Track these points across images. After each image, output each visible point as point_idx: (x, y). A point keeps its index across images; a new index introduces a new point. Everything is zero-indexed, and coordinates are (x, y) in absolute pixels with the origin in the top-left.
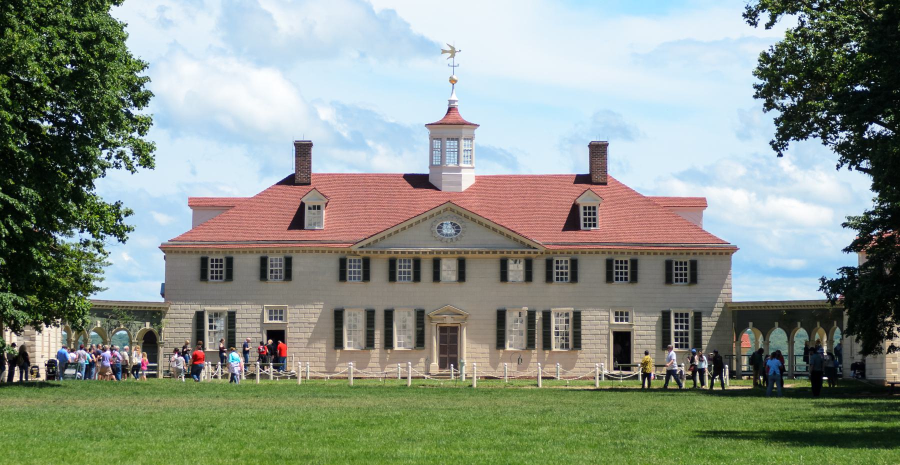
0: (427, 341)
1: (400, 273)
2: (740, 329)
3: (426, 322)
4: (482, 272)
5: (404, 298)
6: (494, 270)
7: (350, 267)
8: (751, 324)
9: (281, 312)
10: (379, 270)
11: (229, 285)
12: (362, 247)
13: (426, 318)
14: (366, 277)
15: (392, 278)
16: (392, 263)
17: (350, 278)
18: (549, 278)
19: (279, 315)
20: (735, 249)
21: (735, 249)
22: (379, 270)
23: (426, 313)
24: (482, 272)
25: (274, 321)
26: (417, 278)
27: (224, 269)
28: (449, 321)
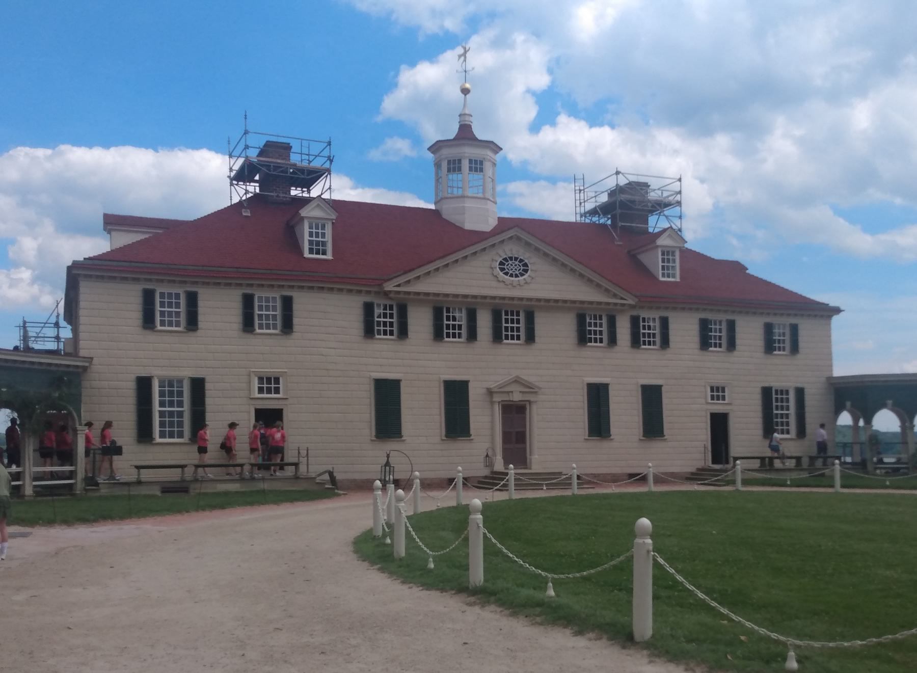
4: (556, 331)
6: (566, 326)
8: (848, 404)
9: (277, 380)
10: (420, 321)
11: (192, 338)
12: (399, 286)
14: (403, 332)
15: (438, 334)
16: (438, 313)
18: (636, 342)
20: (837, 311)
21: (837, 311)
22: (420, 321)
24: (556, 331)
26: (472, 336)
27: (158, 308)
28: (517, 397)
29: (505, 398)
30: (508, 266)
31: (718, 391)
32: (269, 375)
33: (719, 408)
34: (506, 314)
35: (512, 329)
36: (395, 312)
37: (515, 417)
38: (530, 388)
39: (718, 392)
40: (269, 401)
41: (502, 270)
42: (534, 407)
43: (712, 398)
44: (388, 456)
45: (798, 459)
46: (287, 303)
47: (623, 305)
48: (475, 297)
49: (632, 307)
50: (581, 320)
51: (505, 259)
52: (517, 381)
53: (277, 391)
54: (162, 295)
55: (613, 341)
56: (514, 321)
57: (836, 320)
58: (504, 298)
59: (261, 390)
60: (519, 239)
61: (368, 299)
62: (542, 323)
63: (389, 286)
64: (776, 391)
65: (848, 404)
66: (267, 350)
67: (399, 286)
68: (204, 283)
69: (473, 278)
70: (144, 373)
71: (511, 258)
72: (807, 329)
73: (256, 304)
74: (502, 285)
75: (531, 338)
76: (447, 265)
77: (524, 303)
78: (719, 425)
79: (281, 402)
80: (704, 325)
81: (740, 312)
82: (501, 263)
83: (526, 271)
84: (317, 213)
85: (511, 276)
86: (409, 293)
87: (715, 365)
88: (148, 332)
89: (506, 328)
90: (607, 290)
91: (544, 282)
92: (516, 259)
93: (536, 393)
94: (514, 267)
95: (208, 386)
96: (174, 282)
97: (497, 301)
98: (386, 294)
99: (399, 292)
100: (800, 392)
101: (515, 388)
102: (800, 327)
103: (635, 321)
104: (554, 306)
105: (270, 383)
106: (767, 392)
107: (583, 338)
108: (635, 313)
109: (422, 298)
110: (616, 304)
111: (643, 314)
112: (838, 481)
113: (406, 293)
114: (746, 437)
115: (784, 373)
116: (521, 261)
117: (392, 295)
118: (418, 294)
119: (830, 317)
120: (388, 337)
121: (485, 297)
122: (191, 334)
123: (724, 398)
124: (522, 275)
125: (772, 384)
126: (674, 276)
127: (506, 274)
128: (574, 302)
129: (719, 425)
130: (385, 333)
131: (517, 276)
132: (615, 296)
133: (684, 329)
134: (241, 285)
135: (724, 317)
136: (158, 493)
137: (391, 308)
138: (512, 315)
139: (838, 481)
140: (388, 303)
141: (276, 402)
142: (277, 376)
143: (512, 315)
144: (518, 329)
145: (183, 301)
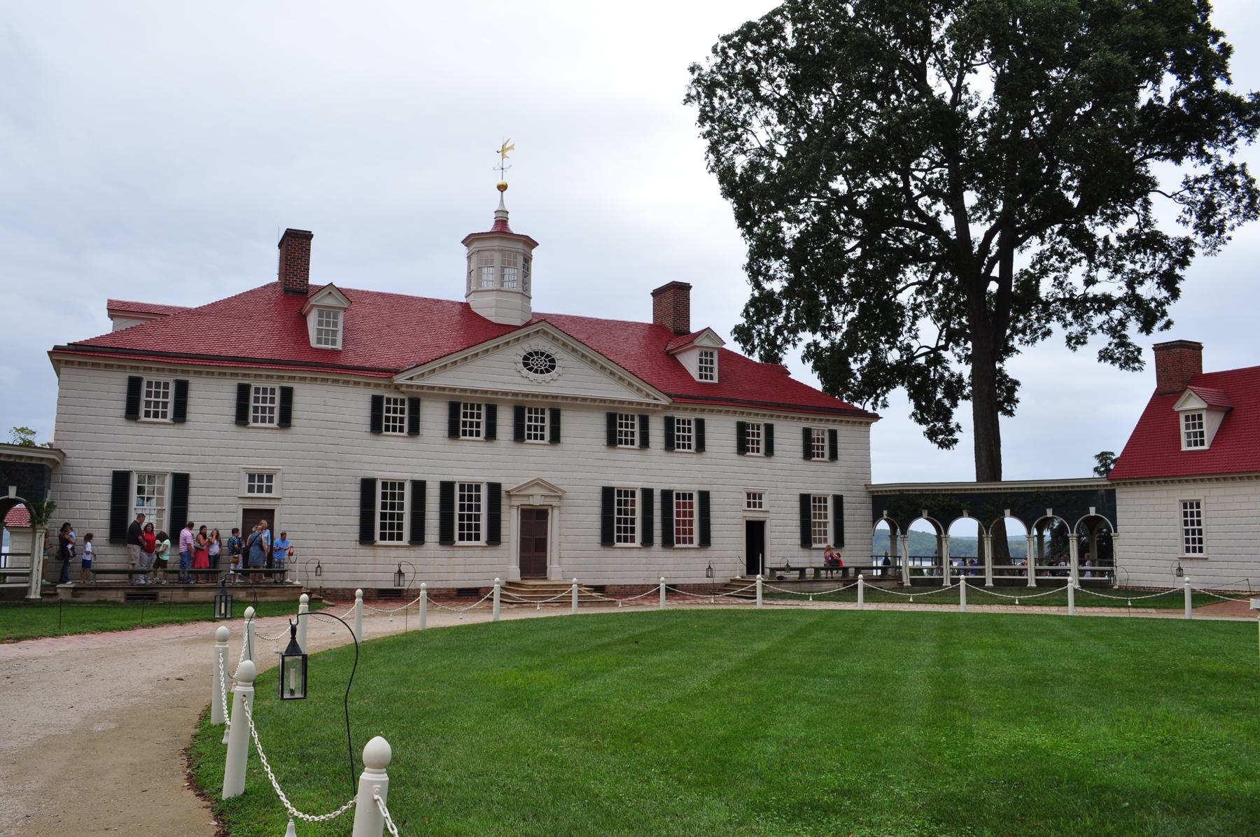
0: (504, 531)
1: (465, 424)
2: (876, 518)
3: (504, 501)
4: (584, 431)
5: (472, 462)
6: (596, 426)
7: (388, 410)
8: (885, 512)
9: (270, 478)
10: (434, 417)
12: (411, 379)
13: (503, 493)
14: (414, 430)
15: (454, 432)
16: (454, 409)
17: (464, 433)
18: (670, 445)
19: (265, 484)
20: (876, 417)
22: (434, 417)
23: (504, 488)
24: (584, 431)
25: (256, 494)
26: (491, 435)
28: (537, 501)
29: (526, 501)
30: (534, 362)
31: (684, 498)
32: (260, 472)
33: (755, 515)
34: (530, 412)
35: (471, 425)
36: (406, 407)
37: (535, 520)
38: (556, 493)
39: (754, 499)
40: (260, 501)
41: (525, 365)
42: (556, 512)
43: (749, 505)
44: (400, 565)
45: (802, 570)
46: (287, 394)
47: (657, 405)
48: (496, 393)
49: (667, 408)
50: (611, 419)
51: (530, 354)
52: (538, 483)
53: (269, 489)
54: (149, 384)
55: (645, 443)
56: (538, 420)
57: (874, 426)
58: (526, 395)
59: (251, 489)
60: (545, 333)
61: (378, 392)
62: (569, 422)
63: (400, 379)
64: (678, 495)
65: (885, 512)
66: (261, 446)
67: (411, 379)
68: (195, 372)
69: (496, 373)
70: (122, 467)
71: (537, 353)
72: (846, 434)
73: (252, 395)
74: (526, 381)
75: (555, 438)
76: (466, 359)
77: (550, 400)
78: (755, 533)
79: (273, 502)
80: (742, 429)
81: (712, 411)
82: (525, 358)
83: (553, 367)
84: (329, 301)
85: (536, 372)
86: (422, 387)
87: (753, 471)
88: (132, 424)
89: (465, 423)
90: (639, 390)
91: (572, 378)
92: (542, 354)
93: (560, 497)
94: (538, 363)
95: (192, 483)
96: (163, 370)
97: (520, 398)
98: (397, 388)
99: (411, 386)
100: (838, 500)
101: (536, 491)
102: (707, 423)
103: (669, 422)
104: (583, 404)
105: (260, 480)
106: (608, 493)
107: (612, 441)
108: (669, 414)
109: (437, 392)
110: (648, 405)
111: (679, 415)
112: (575, 600)
113: (418, 387)
114: (782, 546)
115: (822, 479)
116: (548, 356)
117: (403, 389)
118: (433, 388)
119: (868, 424)
120: (398, 433)
121: (506, 394)
122: (177, 426)
123: (760, 506)
124: (548, 371)
125: (809, 492)
126: (712, 378)
127: (530, 369)
128: (604, 401)
129: (755, 533)
130: (394, 429)
131: (542, 372)
132: (648, 395)
133: (721, 430)
134: (237, 375)
135: (762, 421)
136: (123, 600)
137: (403, 402)
138: (536, 413)
139: (575, 600)
140: (399, 396)
141: (267, 502)
142: (269, 472)
143: (536, 413)
144: (478, 425)
145: (171, 391)
